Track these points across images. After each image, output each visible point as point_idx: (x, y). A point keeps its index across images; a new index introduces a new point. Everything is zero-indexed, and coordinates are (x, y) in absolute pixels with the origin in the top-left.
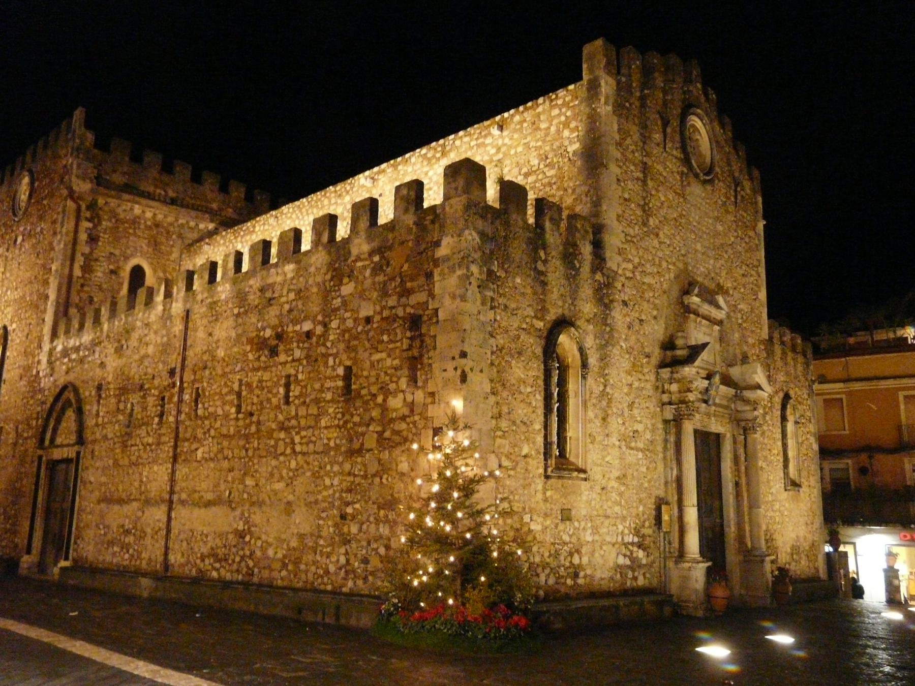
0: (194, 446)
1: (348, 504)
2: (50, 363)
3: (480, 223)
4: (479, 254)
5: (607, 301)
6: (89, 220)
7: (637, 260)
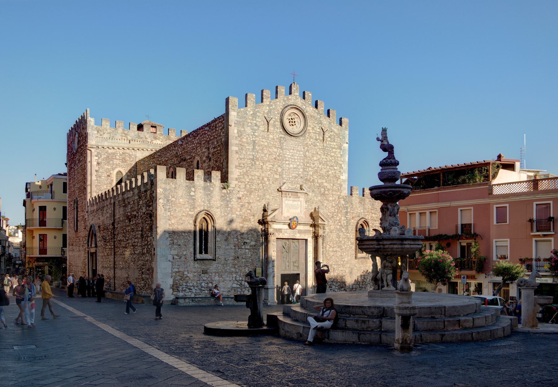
0: (118, 250)
1: (143, 269)
2: (88, 215)
4: (163, 195)
5: (228, 199)
6: (96, 156)
7: (248, 180)
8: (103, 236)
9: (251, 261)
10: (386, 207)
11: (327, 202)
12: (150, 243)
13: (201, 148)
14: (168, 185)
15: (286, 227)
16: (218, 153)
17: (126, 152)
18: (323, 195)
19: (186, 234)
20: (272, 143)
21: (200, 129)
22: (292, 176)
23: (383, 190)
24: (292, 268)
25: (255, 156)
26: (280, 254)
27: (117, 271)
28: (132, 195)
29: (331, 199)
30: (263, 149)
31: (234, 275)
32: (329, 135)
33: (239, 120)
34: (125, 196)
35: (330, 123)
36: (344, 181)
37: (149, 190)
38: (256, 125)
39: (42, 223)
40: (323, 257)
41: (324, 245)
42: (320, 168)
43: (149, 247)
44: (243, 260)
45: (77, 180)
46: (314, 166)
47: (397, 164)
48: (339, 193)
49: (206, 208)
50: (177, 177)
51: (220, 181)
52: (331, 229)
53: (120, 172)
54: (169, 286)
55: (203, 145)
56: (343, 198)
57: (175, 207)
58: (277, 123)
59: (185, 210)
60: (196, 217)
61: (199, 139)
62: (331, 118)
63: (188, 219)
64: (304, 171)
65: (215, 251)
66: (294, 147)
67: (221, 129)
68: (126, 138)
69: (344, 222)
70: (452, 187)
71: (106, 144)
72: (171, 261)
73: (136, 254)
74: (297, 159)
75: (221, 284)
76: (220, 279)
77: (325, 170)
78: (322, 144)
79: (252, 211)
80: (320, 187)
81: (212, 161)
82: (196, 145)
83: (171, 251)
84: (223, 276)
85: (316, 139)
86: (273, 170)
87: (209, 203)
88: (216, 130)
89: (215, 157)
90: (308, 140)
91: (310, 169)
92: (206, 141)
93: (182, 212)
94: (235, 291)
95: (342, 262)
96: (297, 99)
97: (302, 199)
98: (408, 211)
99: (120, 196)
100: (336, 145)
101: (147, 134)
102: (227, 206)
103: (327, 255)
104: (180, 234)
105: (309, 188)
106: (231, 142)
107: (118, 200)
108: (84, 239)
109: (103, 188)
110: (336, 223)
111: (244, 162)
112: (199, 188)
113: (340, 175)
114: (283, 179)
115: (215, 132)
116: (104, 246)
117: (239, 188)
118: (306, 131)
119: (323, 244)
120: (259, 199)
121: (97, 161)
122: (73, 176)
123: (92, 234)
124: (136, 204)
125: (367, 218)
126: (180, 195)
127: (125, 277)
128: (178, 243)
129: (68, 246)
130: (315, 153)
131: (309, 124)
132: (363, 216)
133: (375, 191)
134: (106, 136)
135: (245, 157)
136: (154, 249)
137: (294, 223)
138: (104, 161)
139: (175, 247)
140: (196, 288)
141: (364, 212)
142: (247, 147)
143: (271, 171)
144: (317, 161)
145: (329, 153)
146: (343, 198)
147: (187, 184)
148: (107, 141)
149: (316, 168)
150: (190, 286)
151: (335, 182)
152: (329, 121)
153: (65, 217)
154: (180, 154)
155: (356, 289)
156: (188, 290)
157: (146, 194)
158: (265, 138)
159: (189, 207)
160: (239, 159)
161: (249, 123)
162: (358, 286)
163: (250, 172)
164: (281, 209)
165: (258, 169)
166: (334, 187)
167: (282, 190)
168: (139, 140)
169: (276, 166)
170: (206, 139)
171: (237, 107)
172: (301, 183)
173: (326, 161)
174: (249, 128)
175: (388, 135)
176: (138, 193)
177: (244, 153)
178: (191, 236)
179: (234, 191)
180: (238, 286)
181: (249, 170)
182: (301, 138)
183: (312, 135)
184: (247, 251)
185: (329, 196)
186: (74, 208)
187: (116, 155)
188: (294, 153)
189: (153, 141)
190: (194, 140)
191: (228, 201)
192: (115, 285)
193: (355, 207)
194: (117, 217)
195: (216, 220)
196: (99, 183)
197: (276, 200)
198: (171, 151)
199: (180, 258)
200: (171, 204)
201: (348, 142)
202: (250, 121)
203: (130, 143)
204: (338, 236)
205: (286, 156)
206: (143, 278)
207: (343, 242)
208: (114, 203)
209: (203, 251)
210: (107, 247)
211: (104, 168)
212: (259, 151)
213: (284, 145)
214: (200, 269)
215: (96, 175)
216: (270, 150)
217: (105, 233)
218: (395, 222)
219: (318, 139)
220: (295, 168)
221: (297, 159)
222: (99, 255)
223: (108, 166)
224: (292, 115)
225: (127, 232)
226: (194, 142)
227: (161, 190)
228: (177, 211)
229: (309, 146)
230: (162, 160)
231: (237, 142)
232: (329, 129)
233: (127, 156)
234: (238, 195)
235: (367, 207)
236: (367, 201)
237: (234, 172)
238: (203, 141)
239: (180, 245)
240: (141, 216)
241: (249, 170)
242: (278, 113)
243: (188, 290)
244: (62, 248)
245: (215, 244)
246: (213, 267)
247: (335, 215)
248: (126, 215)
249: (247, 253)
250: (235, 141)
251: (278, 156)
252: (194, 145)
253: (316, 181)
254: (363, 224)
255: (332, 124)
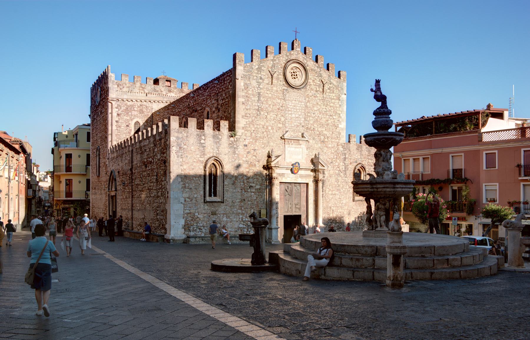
0: (136, 193)
1: (157, 211)
2: (109, 162)
3: (176, 134)
4: (176, 143)
5: (235, 146)
7: (253, 129)
8: (122, 181)
9: (256, 203)
10: (379, 152)
11: (326, 149)
12: (164, 186)
13: (210, 99)
14: (181, 133)
15: (289, 172)
16: (226, 104)
17: (144, 104)
18: (323, 142)
19: (197, 179)
20: (276, 95)
21: (210, 82)
22: (295, 125)
23: (377, 137)
24: (294, 210)
25: (260, 106)
26: (283, 197)
27: (134, 212)
28: (148, 143)
29: (330, 146)
30: (267, 100)
31: (241, 216)
32: (328, 87)
33: (245, 74)
34: (142, 144)
35: (329, 76)
36: (342, 129)
37: (163, 138)
38: (261, 78)
39: (68, 169)
40: (323, 200)
41: (324, 188)
42: (320, 118)
43: (164, 190)
44: (249, 203)
45: (99, 130)
46: (315, 115)
47: (390, 113)
48: (337, 141)
49: (215, 155)
50: (189, 126)
51: (228, 130)
52: (331, 173)
53: (137, 123)
54: (181, 226)
55: (213, 97)
56: (342, 145)
57: (187, 153)
58: (280, 76)
59: (196, 157)
60: (206, 162)
61: (209, 91)
62: (330, 71)
63: (198, 165)
64: (305, 119)
65: (224, 194)
66: (296, 98)
67: (229, 83)
68: (143, 92)
69: (342, 168)
70: (444, 134)
71: (125, 97)
72: (183, 203)
73: (151, 197)
74: (299, 109)
75: (228, 224)
76: (228, 219)
77: (325, 120)
78: (322, 95)
79: (257, 157)
80: (320, 135)
81: (221, 111)
82: (206, 97)
83: (183, 194)
84: (231, 217)
85: (316, 91)
86: (277, 119)
87: (218, 150)
88: (224, 84)
89: (223, 108)
90: (309, 92)
91: (311, 118)
92: (216, 93)
93: (193, 158)
94: (241, 231)
95: (340, 205)
96: (298, 54)
97: (304, 145)
98: (403, 157)
99: (138, 144)
100: (335, 96)
101: (162, 87)
102: (234, 153)
103: (327, 198)
104: (192, 178)
105: (310, 136)
106: (238, 95)
107: (136, 148)
108: (105, 183)
109: (122, 137)
110: (335, 168)
111: (250, 112)
112: (208, 136)
113: (338, 124)
114: (286, 128)
115: (223, 85)
116: (123, 190)
117: (245, 136)
118: (307, 83)
119: (323, 187)
120: (263, 146)
121: (117, 112)
122: (96, 126)
123: (112, 179)
124: (152, 151)
125: (363, 163)
126: (191, 143)
127: (142, 217)
128: (190, 187)
129: (91, 190)
130: (315, 103)
131: (310, 77)
132: (360, 162)
133: (369, 139)
134: (125, 89)
135: (251, 108)
136: (168, 192)
137: (296, 168)
138: (124, 113)
139: (186, 190)
140: (205, 228)
141: (361, 158)
142: (253, 99)
143: (275, 121)
144: (317, 111)
145: (328, 104)
146: (342, 145)
147: (198, 133)
148: (126, 94)
149: (316, 118)
150: (200, 226)
151: (334, 130)
152: (329, 74)
153: (88, 164)
154: (192, 106)
155: (354, 229)
156: (199, 230)
157: (161, 142)
158: (269, 90)
159: (200, 154)
160: (245, 110)
161: (254, 76)
162: (356, 226)
163: (256, 122)
164: (283, 155)
165: (263, 119)
166: (333, 135)
167: (285, 138)
168: (155, 93)
169: (280, 116)
170: (215, 92)
171: (244, 62)
172: (302, 132)
173: (326, 110)
174: (254, 81)
175: (381, 87)
176: (154, 142)
177: (250, 104)
178: (201, 180)
179: (240, 139)
180: (244, 226)
181: (254, 120)
182: (303, 90)
183: (313, 87)
184: (253, 194)
185: (328, 143)
186: (97, 156)
187: (134, 106)
188: (296, 104)
189: (167, 93)
190: (204, 93)
191: (235, 148)
192: (132, 225)
193: (352, 153)
194: (135, 163)
195: (224, 165)
196: (119, 132)
197: (279, 147)
198: (183, 103)
199: (191, 201)
200: (183, 151)
201: (346, 93)
202: (255, 75)
203: (146, 96)
204: (337, 181)
205: (289, 106)
206: (157, 219)
207: (341, 186)
208: (132, 150)
209: (212, 194)
210: (125, 191)
211: (123, 119)
212: (264, 102)
213: (287, 96)
214: (209, 211)
215: (116, 126)
216: (274, 101)
217: (124, 178)
218: (388, 167)
219: (319, 91)
220: (297, 117)
221: (299, 109)
222: (119, 198)
223: (127, 117)
224: (294, 69)
225: (143, 177)
226: (204, 94)
227: (175, 138)
228: (189, 158)
229: (310, 97)
230: (176, 111)
231: (244, 94)
232: (328, 82)
233: (144, 107)
234: (244, 143)
235: (364, 154)
236: (364, 148)
237: (241, 122)
238: (212, 93)
239: (191, 189)
240: (156, 162)
241: (254, 120)
242: (281, 68)
243: (198, 230)
244: (86, 191)
245: (224, 188)
246: (221, 209)
247: (334, 161)
248: (143, 161)
249: (253, 196)
250: (242, 93)
251: (281, 106)
252: (204, 98)
253: (316, 129)
254: (360, 169)
255: (331, 77)
